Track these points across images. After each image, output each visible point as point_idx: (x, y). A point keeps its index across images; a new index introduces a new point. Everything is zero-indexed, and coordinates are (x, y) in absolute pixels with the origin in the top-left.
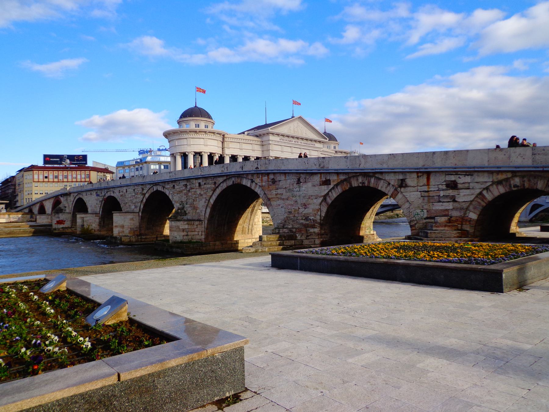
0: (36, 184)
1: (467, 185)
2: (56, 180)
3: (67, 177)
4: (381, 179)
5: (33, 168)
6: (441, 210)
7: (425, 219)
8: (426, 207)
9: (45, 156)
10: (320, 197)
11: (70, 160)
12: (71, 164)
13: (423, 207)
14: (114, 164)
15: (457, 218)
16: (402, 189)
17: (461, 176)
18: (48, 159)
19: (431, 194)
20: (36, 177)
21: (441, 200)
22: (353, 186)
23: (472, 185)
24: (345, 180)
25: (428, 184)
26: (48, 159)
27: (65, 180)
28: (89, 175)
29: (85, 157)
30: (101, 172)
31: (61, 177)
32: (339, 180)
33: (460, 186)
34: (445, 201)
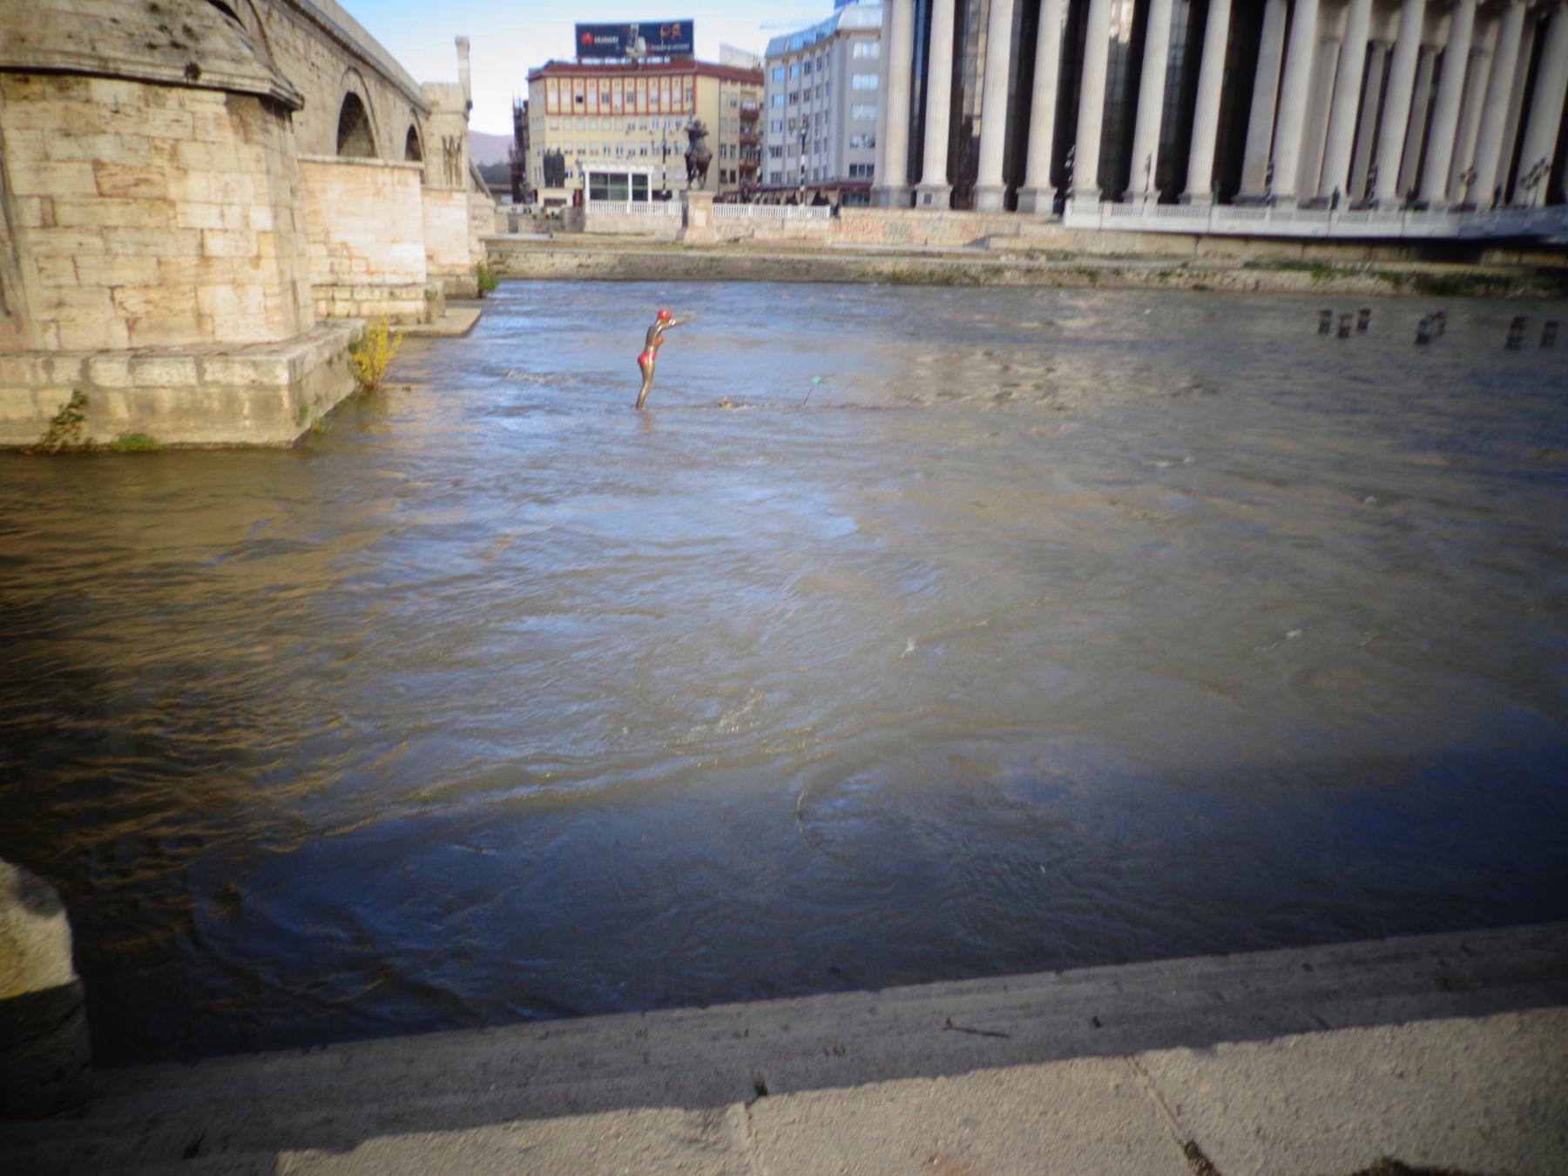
0: (554, 122)
2: (605, 108)
3: (633, 98)
5: (555, 69)
9: (581, 30)
11: (648, 41)
12: (650, 53)
14: (761, 51)
18: (591, 39)
20: (552, 98)
26: (591, 39)
27: (629, 108)
28: (694, 90)
29: (686, 29)
30: (734, 80)
31: (617, 100)
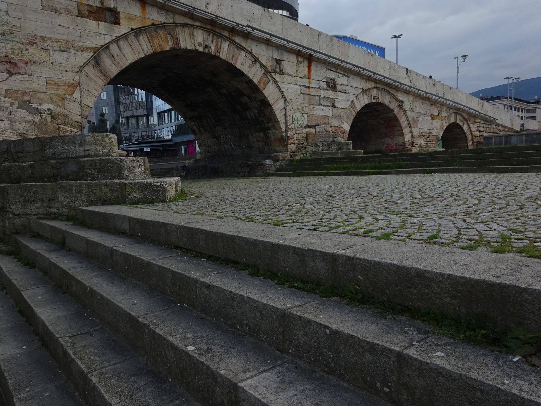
1: (344, 88)
4: (243, 49)
6: (322, 116)
7: (305, 127)
8: (306, 110)
10: (83, 49)
13: (303, 110)
15: (336, 128)
16: (278, 77)
17: (340, 76)
19: (313, 92)
21: (322, 102)
22: (183, 46)
23: (349, 89)
24: (163, 26)
25: (309, 78)
32: (148, 23)
33: (339, 87)
34: (326, 104)
